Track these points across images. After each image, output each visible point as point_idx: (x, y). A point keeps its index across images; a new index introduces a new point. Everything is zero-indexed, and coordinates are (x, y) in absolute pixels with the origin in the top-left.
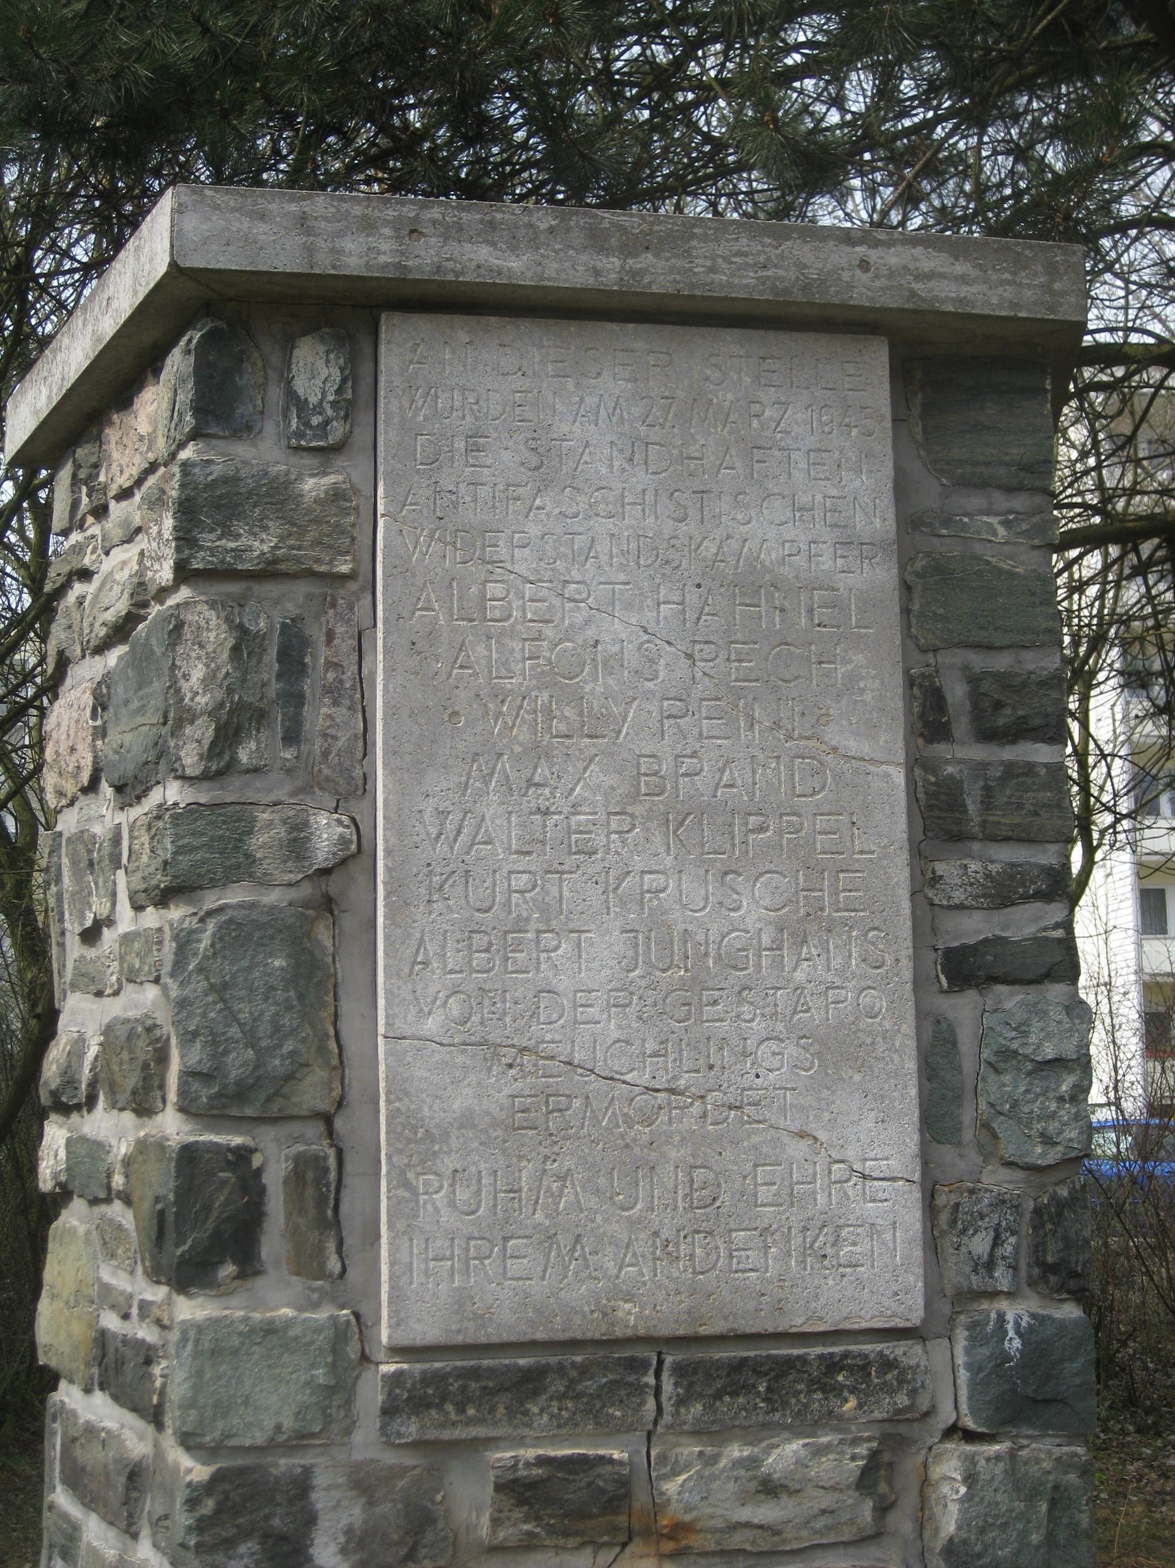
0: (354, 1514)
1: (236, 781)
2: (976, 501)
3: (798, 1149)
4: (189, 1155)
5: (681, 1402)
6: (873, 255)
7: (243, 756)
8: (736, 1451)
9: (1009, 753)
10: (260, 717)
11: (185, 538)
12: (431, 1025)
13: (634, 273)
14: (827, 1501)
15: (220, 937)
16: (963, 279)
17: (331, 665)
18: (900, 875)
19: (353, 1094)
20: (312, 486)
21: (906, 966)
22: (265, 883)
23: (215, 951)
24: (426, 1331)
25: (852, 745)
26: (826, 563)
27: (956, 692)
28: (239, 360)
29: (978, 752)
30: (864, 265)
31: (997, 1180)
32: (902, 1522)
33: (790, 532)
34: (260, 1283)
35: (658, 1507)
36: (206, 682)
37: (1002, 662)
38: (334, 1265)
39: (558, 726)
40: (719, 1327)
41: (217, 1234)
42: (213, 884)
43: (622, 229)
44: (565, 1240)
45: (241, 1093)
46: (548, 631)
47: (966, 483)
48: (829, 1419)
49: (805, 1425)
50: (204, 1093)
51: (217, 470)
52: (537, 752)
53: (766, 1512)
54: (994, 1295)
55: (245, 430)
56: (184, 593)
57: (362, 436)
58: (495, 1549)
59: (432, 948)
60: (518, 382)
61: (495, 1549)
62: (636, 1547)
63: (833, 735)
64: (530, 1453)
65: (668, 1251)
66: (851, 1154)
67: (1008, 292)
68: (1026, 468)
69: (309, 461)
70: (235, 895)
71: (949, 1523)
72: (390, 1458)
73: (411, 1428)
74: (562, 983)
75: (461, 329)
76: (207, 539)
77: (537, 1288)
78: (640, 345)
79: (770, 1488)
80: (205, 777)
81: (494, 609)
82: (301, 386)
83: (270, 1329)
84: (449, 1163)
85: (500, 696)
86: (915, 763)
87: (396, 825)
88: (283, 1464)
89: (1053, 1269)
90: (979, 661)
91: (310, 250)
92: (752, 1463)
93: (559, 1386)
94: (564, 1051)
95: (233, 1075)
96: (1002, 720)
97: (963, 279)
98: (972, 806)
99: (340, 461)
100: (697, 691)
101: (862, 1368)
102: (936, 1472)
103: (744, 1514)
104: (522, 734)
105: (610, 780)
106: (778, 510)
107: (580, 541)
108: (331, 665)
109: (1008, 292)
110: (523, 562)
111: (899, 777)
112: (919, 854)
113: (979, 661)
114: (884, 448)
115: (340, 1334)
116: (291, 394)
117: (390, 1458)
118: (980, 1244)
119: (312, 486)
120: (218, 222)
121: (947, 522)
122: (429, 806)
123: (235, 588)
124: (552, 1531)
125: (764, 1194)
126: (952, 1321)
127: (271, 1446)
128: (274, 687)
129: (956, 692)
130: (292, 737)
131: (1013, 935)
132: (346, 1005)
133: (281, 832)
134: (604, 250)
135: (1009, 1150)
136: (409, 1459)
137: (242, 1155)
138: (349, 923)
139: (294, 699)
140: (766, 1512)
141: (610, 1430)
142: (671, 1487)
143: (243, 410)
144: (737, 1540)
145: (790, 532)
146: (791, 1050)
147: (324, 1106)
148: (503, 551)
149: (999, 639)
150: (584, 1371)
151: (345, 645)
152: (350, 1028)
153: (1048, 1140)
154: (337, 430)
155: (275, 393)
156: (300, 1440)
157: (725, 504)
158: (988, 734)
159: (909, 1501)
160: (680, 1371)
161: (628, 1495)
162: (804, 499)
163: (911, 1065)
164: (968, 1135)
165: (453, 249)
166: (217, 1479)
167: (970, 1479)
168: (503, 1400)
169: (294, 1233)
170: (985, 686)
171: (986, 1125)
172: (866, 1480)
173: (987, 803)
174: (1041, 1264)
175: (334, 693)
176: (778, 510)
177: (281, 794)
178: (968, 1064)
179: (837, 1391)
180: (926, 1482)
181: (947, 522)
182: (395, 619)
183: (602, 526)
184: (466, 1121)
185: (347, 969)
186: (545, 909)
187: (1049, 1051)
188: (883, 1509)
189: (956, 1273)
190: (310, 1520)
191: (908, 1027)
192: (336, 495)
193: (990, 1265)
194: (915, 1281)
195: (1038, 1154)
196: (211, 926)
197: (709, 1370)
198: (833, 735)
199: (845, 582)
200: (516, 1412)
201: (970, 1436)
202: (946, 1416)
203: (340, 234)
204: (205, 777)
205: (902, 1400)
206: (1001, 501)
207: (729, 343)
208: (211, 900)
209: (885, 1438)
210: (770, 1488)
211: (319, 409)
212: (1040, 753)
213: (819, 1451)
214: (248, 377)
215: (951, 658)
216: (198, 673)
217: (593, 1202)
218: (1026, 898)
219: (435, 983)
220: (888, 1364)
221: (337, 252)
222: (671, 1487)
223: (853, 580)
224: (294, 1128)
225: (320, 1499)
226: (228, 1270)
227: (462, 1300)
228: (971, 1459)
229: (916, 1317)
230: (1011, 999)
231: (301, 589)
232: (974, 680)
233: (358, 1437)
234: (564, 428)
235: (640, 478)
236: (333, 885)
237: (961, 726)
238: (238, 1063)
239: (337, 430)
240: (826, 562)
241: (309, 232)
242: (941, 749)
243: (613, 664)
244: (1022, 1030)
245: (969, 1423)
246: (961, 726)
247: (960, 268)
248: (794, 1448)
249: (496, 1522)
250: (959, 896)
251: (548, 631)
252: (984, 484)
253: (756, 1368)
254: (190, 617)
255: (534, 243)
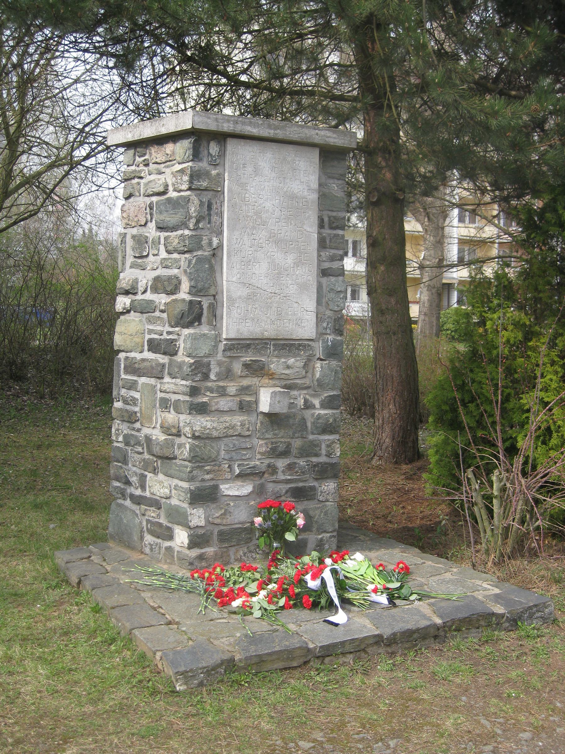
0: (217, 369)
1: (199, 231)
2: (331, 181)
3: (296, 305)
4: (191, 302)
5: (274, 351)
6: (319, 132)
7: (200, 226)
8: (283, 360)
9: (335, 232)
10: (204, 218)
11: (191, 182)
12: (234, 279)
13: (276, 134)
14: (298, 370)
15: (196, 261)
16: (335, 138)
17: (216, 209)
18: (315, 254)
19: (219, 292)
20: (214, 172)
21: (316, 272)
22: (205, 251)
23: (196, 264)
24: (232, 336)
25: (308, 229)
26: (306, 193)
27: (326, 219)
28: (200, 145)
29: (329, 231)
30: (317, 134)
31: (328, 313)
32: (309, 375)
33: (300, 187)
34: (201, 326)
35: (269, 370)
36: (195, 211)
37: (334, 214)
38: (214, 323)
39: (258, 223)
40: (281, 337)
41: (195, 317)
42: (196, 251)
43: (274, 124)
44: (256, 320)
45: (200, 291)
46: (256, 204)
47: (330, 177)
48: (299, 355)
49: (295, 356)
50: (194, 290)
51: (197, 168)
52: (254, 228)
53: (287, 372)
54: (327, 334)
55: (201, 160)
56: (188, 193)
57: (222, 162)
58: (241, 377)
59: (235, 264)
60: (252, 154)
61: (241, 377)
62: (265, 377)
63: (305, 227)
64: (248, 359)
65: (273, 323)
66: (304, 306)
67: (343, 141)
68: (341, 175)
69: (212, 167)
70: (200, 253)
71: (318, 375)
72: (224, 359)
73: (229, 354)
74: (257, 272)
75: (242, 142)
76: (195, 182)
77: (251, 329)
78: (274, 147)
79: (288, 367)
80: (194, 230)
81: (247, 199)
82: (211, 151)
83: (204, 335)
84: (237, 305)
85: (248, 216)
86: (319, 233)
87: (229, 240)
88: (206, 360)
89: (337, 330)
90: (331, 213)
91: (218, 126)
92: (285, 362)
93: (253, 347)
94: (256, 285)
95: (199, 287)
96: (334, 225)
97: (335, 138)
98: (328, 242)
99: (218, 167)
100: (282, 217)
101: (305, 346)
102: (316, 366)
103: (284, 372)
104: (251, 224)
105: (266, 234)
106: (298, 182)
107: (262, 187)
108: (216, 209)
109: (343, 141)
110: (252, 190)
111: (316, 236)
112: (318, 251)
113: (331, 213)
114: (317, 171)
115: (216, 336)
116: (209, 153)
117: (224, 359)
118: (325, 325)
119: (214, 172)
120: (201, 119)
121: (326, 185)
122: (235, 237)
123: (199, 192)
124: (251, 374)
125: (290, 313)
126: (319, 338)
127: (204, 357)
128: (206, 212)
129: (326, 219)
130: (209, 223)
131: (334, 267)
132: (217, 274)
133: (207, 241)
134: (271, 129)
135: (331, 308)
136: (227, 360)
137: (200, 302)
138: (218, 259)
139: (210, 215)
140: (287, 372)
141: (263, 355)
142: (272, 366)
143: (201, 156)
144: (282, 376)
145: (300, 187)
146: (295, 287)
147: (214, 293)
148: (249, 188)
149: (334, 209)
150: (258, 344)
151: (219, 205)
152: (218, 279)
153: (338, 306)
154: (218, 161)
155: (206, 152)
156: (209, 356)
157: (288, 181)
158: (331, 228)
159: (311, 371)
160: (274, 345)
161: (264, 368)
162: (302, 180)
163: (316, 291)
164: (324, 304)
165: (244, 127)
166: (195, 362)
167: (322, 367)
168: (244, 349)
169: (208, 317)
170: (332, 219)
171: (327, 303)
172: (304, 367)
173: (330, 242)
174: (335, 329)
175: (217, 214)
176: (298, 182)
177: (207, 233)
178: (324, 291)
179: (300, 350)
180: (314, 368)
181: (326, 185)
182: (229, 201)
183: (267, 184)
184: (240, 297)
185: (217, 268)
186: (254, 258)
187: (339, 289)
188: (306, 372)
189: (321, 330)
190: (210, 370)
191: (315, 283)
192: (218, 174)
193: (326, 329)
194: (314, 330)
195: (336, 308)
196: (195, 258)
197: (279, 345)
198: (305, 227)
199: (309, 197)
200: (246, 351)
201: (321, 360)
202: (318, 356)
203: (223, 123)
204: (194, 230)
205: (311, 352)
206: (336, 181)
207: (291, 148)
208: (195, 254)
209: (308, 359)
210: (288, 367)
211: (214, 156)
212: (340, 232)
213: (298, 360)
214: (201, 149)
215: (326, 213)
216: (193, 209)
217: (261, 313)
218: (336, 260)
219: (235, 271)
220: (309, 346)
221: (222, 126)
222: (272, 366)
223: (310, 197)
224: (209, 297)
225: (212, 367)
226: (197, 323)
227: (238, 330)
228: (322, 364)
229: (314, 337)
230: (333, 279)
231: (211, 193)
232: (329, 217)
233: (218, 355)
234: (260, 164)
235: (273, 175)
236: (216, 252)
237: (326, 226)
238: (200, 286)
239: (218, 161)
240: (306, 193)
241: (218, 122)
242: (323, 230)
243: (267, 211)
244: (335, 285)
245: (322, 357)
246: (326, 226)
247: (335, 136)
248: (293, 360)
249: (242, 371)
250: (324, 259)
251: (256, 204)
252: (333, 178)
253: (286, 345)
254: (191, 198)
255: (258, 127)
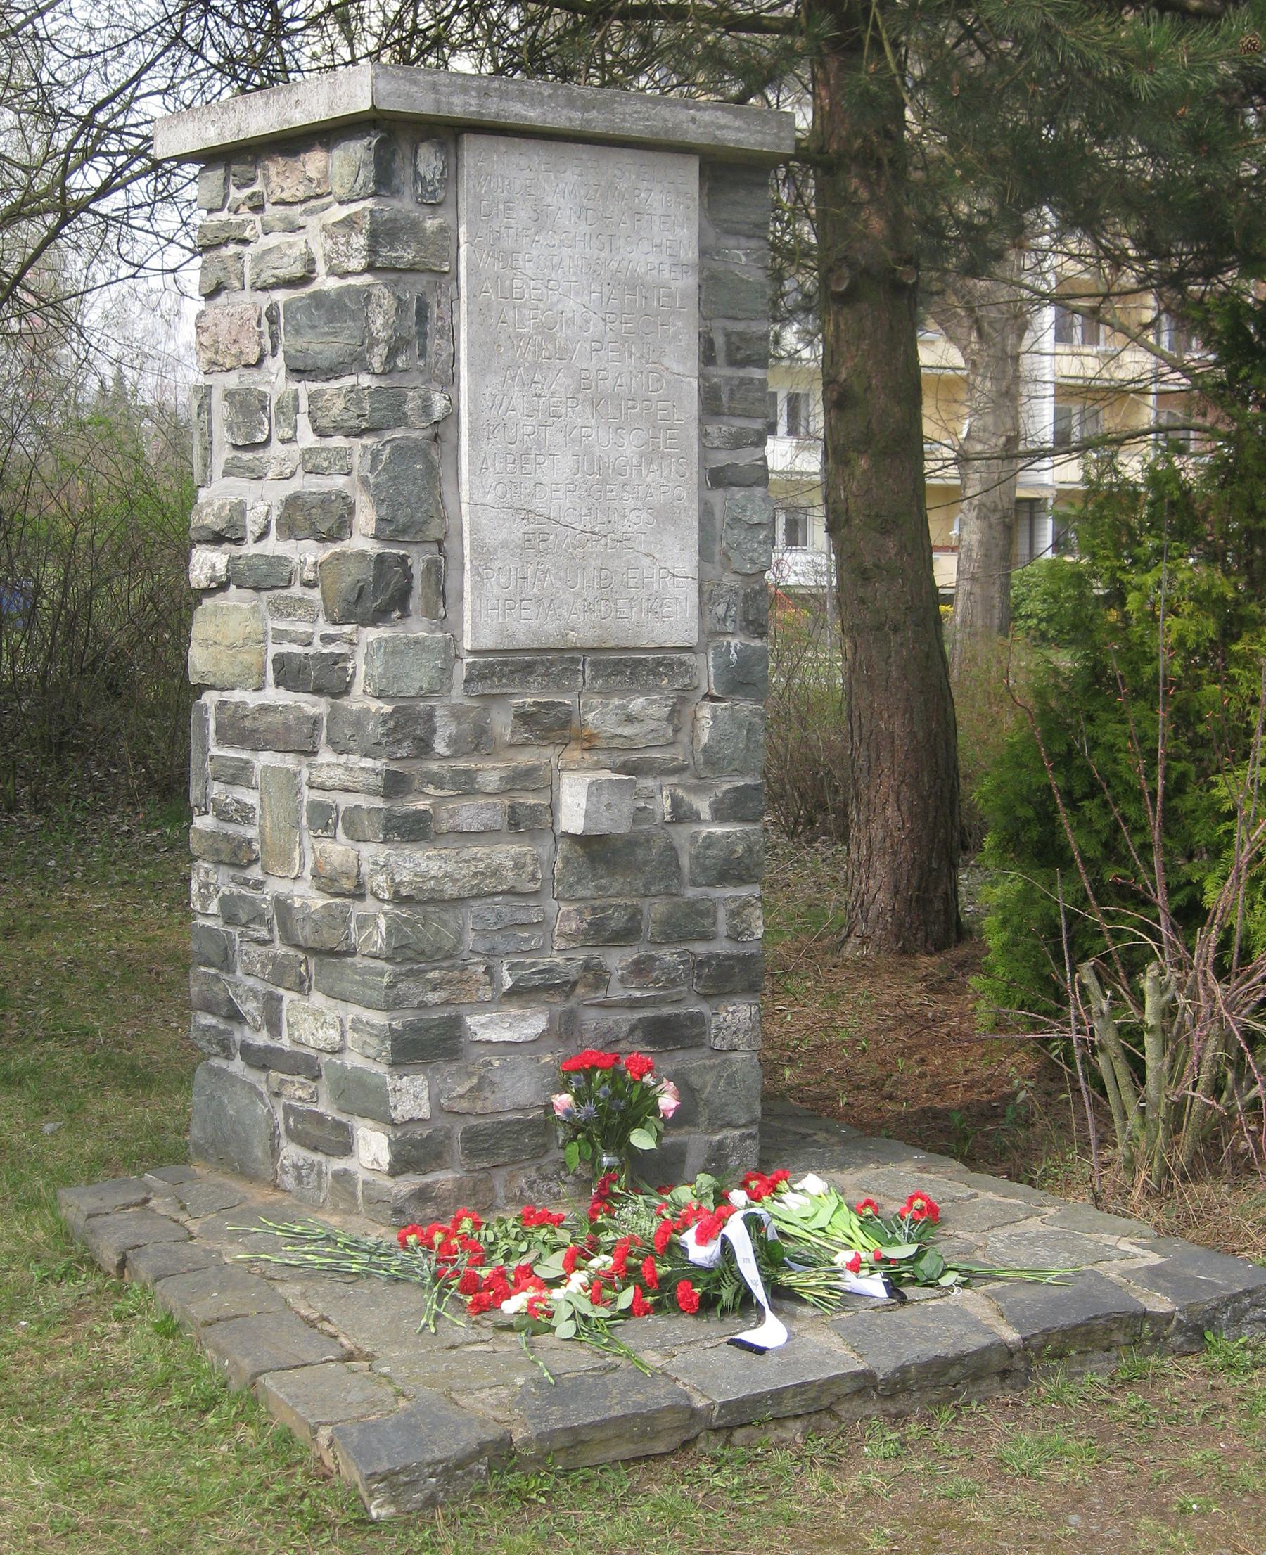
0: (452, 729)
1: (397, 376)
2: (732, 242)
3: (646, 562)
4: (380, 558)
5: (593, 678)
6: (698, 115)
8: (617, 702)
10: (408, 343)
11: (372, 250)
12: (489, 499)
13: (588, 121)
14: (654, 725)
15: (392, 453)
16: (738, 129)
17: (440, 318)
18: (694, 432)
19: (451, 532)
20: (430, 224)
21: (695, 476)
22: (412, 427)
24: (487, 642)
25: (675, 367)
26: (666, 274)
27: (720, 341)
28: (393, 154)
30: (693, 120)
31: (729, 580)
32: (684, 737)
33: (650, 258)
34: (409, 620)
35: (583, 727)
36: (385, 325)
37: (740, 327)
38: (442, 612)
40: (611, 644)
41: (392, 597)
43: (583, 97)
45: (404, 531)
46: (541, 305)
48: (656, 688)
49: (646, 691)
50: (388, 529)
52: (536, 366)
53: (627, 730)
54: (726, 634)
55: (396, 193)
56: (367, 279)
57: (451, 197)
58: (511, 745)
59: (489, 461)
60: (527, 173)
61: (511, 745)
62: (572, 745)
63: (667, 362)
65: (589, 607)
66: (669, 565)
67: (759, 137)
68: (757, 226)
69: (427, 210)
70: (399, 433)
71: (705, 737)
72: (468, 703)
73: (479, 688)
74: (546, 480)
75: (502, 143)
77: (535, 624)
78: (584, 156)
79: (630, 719)
82: (422, 169)
83: (417, 642)
84: (497, 564)
85: (520, 337)
86: (702, 376)
87: (473, 400)
88: (422, 705)
89: (749, 623)
91: (438, 102)
92: (623, 707)
93: (542, 670)
94: (546, 512)
97: (738, 129)
98: (725, 398)
99: (441, 211)
100: (607, 338)
101: (671, 665)
102: (699, 715)
103: (619, 731)
104: (528, 356)
106: (645, 246)
108: (440, 318)
109: (759, 137)
110: (530, 269)
112: (701, 422)
114: (695, 215)
116: (417, 173)
117: (468, 703)
118: (721, 610)
119: (430, 224)
122: (488, 391)
123: (393, 276)
124: (537, 737)
125: (632, 582)
127: (418, 697)
128: (414, 329)
129: (720, 341)
131: (741, 463)
132: (445, 488)
133: (418, 402)
135: (735, 566)
137: (404, 559)
138: (446, 447)
139: (423, 335)
140: (627, 730)
141: (565, 691)
142: (589, 717)
143: (396, 182)
144: (616, 743)
146: (645, 515)
147: (440, 536)
148: (521, 263)
149: (741, 314)
150: (552, 663)
151: (445, 308)
152: (449, 498)
153: (753, 562)
154: (441, 195)
155: (409, 171)
156: (430, 694)
157: (621, 242)
158: (733, 363)
159: (687, 728)
160: (593, 664)
163: (696, 524)
164: (717, 558)
165: (504, 105)
166: (395, 711)
167: (714, 718)
168: (519, 675)
169: (425, 597)
170: (734, 339)
171: (725, 554)
172: (670, 718)
173: (731, 398)
175: (441, 332)
176: (645, 246)
177: (418, 383)
178: (718, 524)
179: (660, 674)
181: (718, 253)
182: (472, 297)
183: (566, 252)
184: (504, 545)
186: (538, 443)
187: (755, 520)
188: (676, 731)
189: (711, 624)
190: (434, 731)
191: (695, 506)
192: (442, 229)
193: (725, 620)
194: (694, 625)
195: (748, 568)
196: (388, 448)
198: (667, 362)
199: (674, 284)
200: (524, 681)
201: (714, 699)
202: (704, 689)
203: (451, 94)
205: (687, 681)
206: (744, 242)
207: (626, 156)
208: (388, 435)
209: (679, 698)
210: (630, 719)
211: (431, 183)
212: (756, 373)
213: (654, 702)
214: (397, 164)
215: (718, 323)
217: (558, 584)
218: (747, 445)
219: (491, 478)
220: (682, 664)
221: (450, 104)
222: (589, 717)
223: (678, 283)
224: (426, 546)
225: (438, 722)
226: (397, 614)
227: (502, 629)
228: (714, 709)
229: (694, 643)
230: (739, 493)
231: (425, 278)
232: (728, 335)
233: (454, 693)
234: (549, 199)
235: (584, 228)
236: (440, 429)
237: (721, 357)
238: (402, 517)
239: (441, 195)
240: (666, 274)
241: (437, 92)
242: (711, 369)
243: (570, 322)
245: (714, 692)
246: (721, 357)
247: (738, 123)
248: (641, 701)
250: (717, 443)
251: (541, 305)
252: (736, 233)
253: (625, 663)
254: (374, 291)
